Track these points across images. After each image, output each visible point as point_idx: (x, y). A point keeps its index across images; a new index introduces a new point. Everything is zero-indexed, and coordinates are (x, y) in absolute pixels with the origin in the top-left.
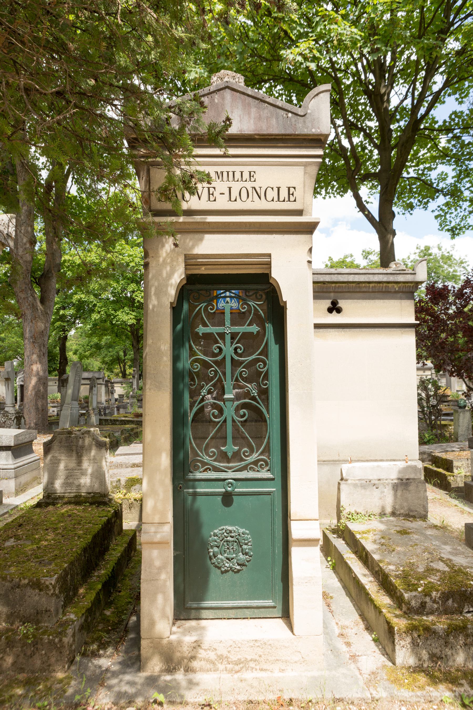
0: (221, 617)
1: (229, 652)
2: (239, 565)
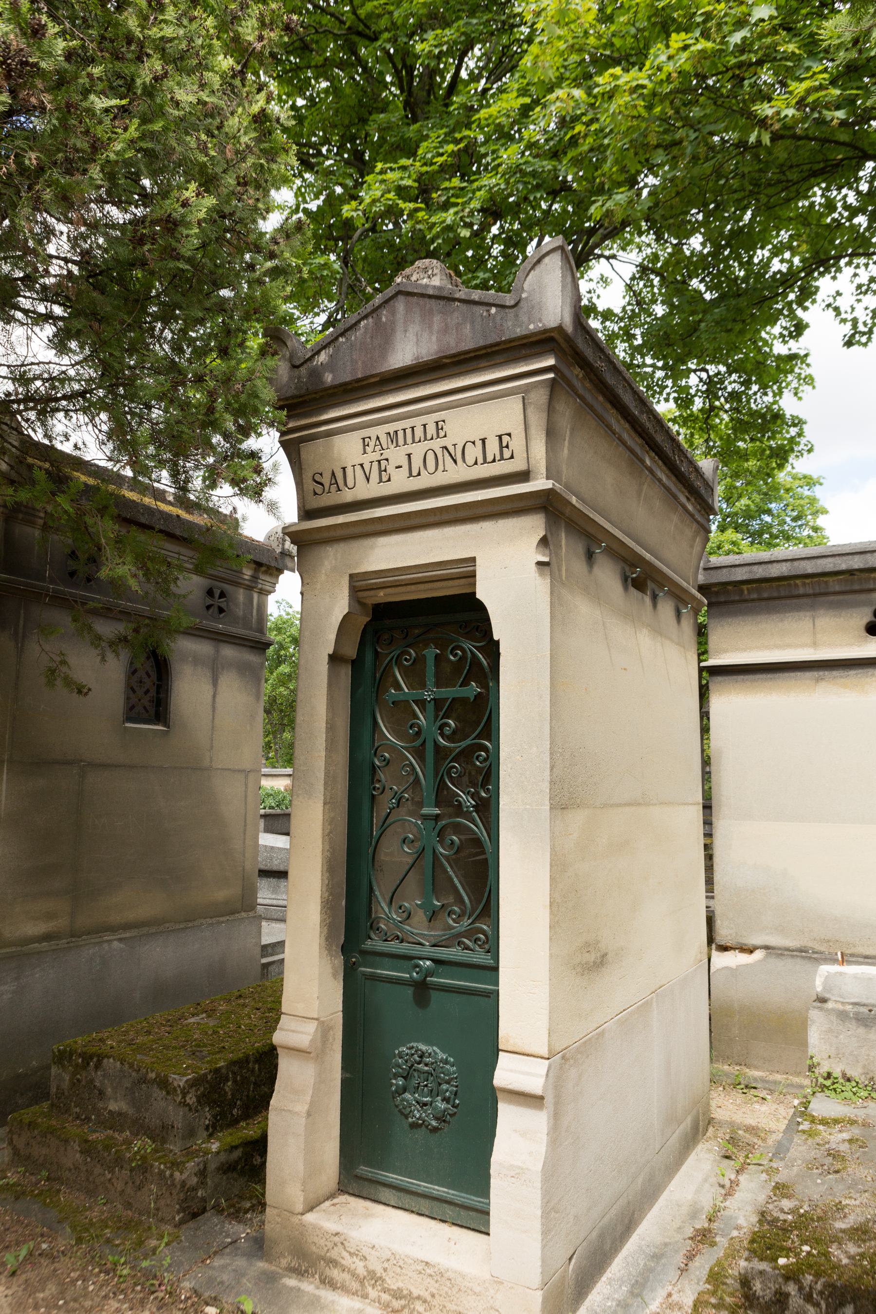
0: (407, 1207)
1: (385, 1270)
2: (436, 1119)
